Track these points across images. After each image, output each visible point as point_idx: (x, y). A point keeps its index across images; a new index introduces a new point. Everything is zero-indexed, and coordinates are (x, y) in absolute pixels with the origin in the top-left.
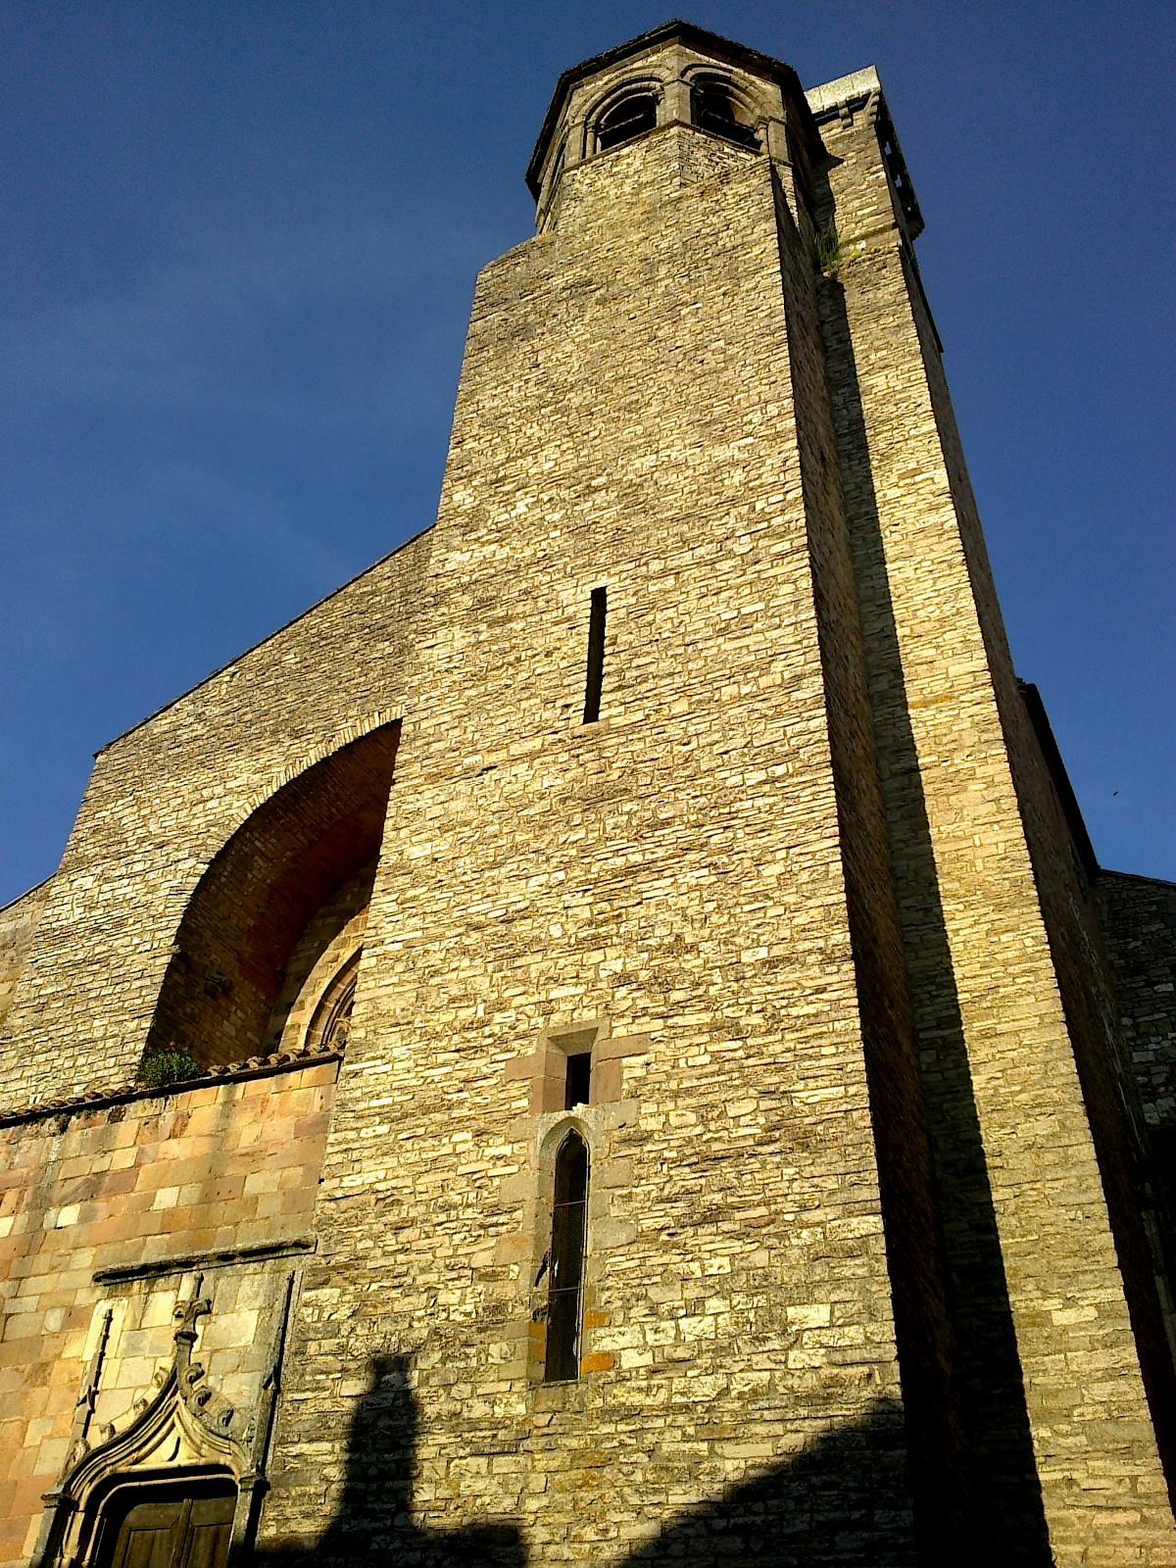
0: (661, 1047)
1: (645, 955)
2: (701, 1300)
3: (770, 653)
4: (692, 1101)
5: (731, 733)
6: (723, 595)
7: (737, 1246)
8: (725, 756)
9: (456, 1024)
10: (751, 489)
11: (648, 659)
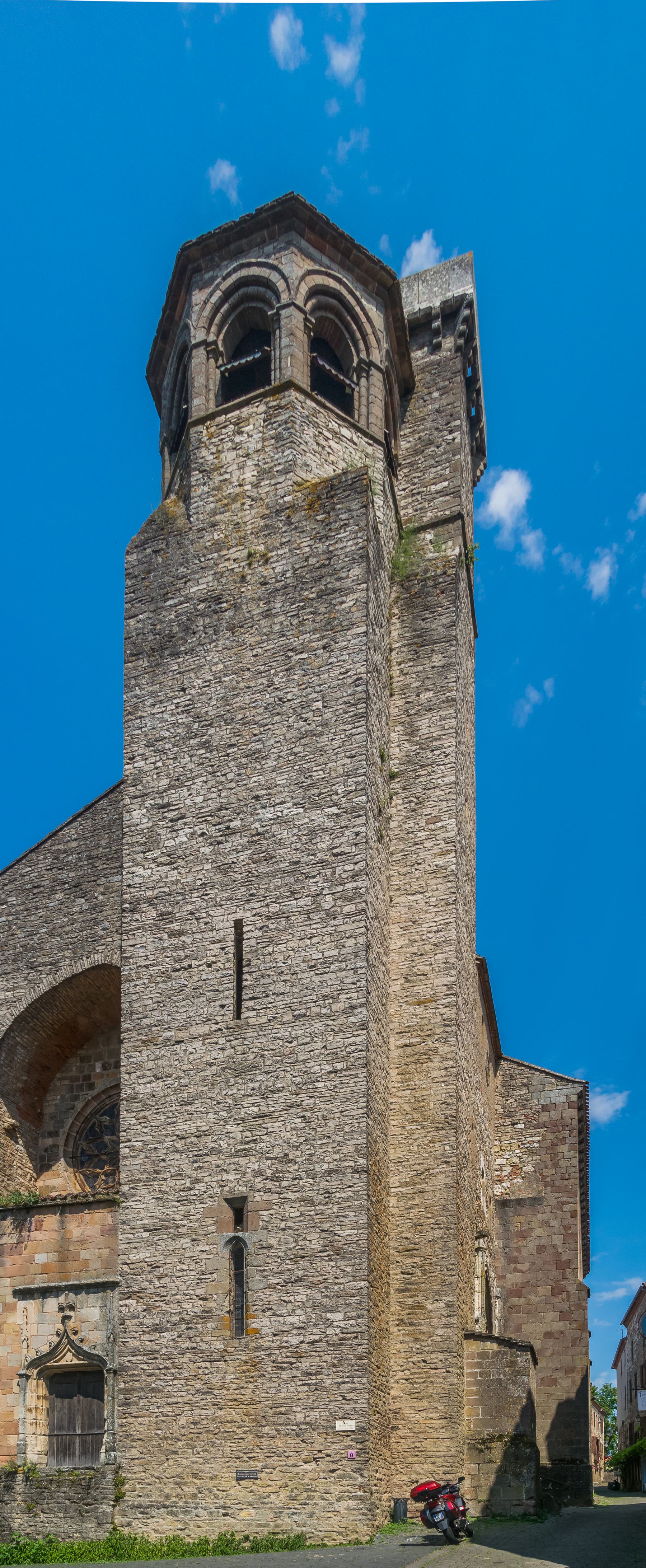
0: (277, 1207)
1: (269, 1162)
2: (293, 1311)
3: (339, 988)
4: (290, 1232)
5: (315, 1039)
6: (314, 940)
7: (309, 1292)
8: (312, 1053)
9: (177, 1187)
10: (335, 855)
11: (270, 981)
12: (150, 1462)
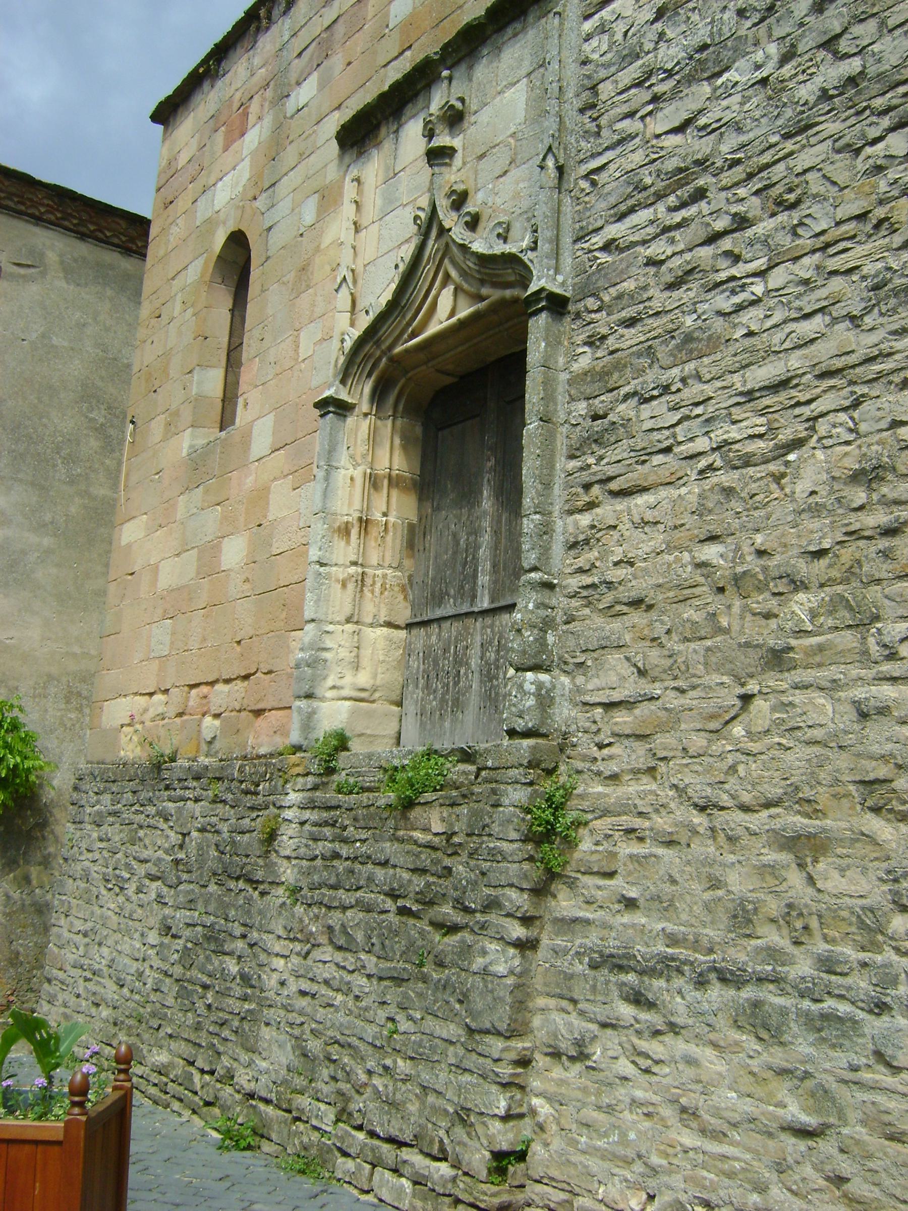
12: (673, 719)
